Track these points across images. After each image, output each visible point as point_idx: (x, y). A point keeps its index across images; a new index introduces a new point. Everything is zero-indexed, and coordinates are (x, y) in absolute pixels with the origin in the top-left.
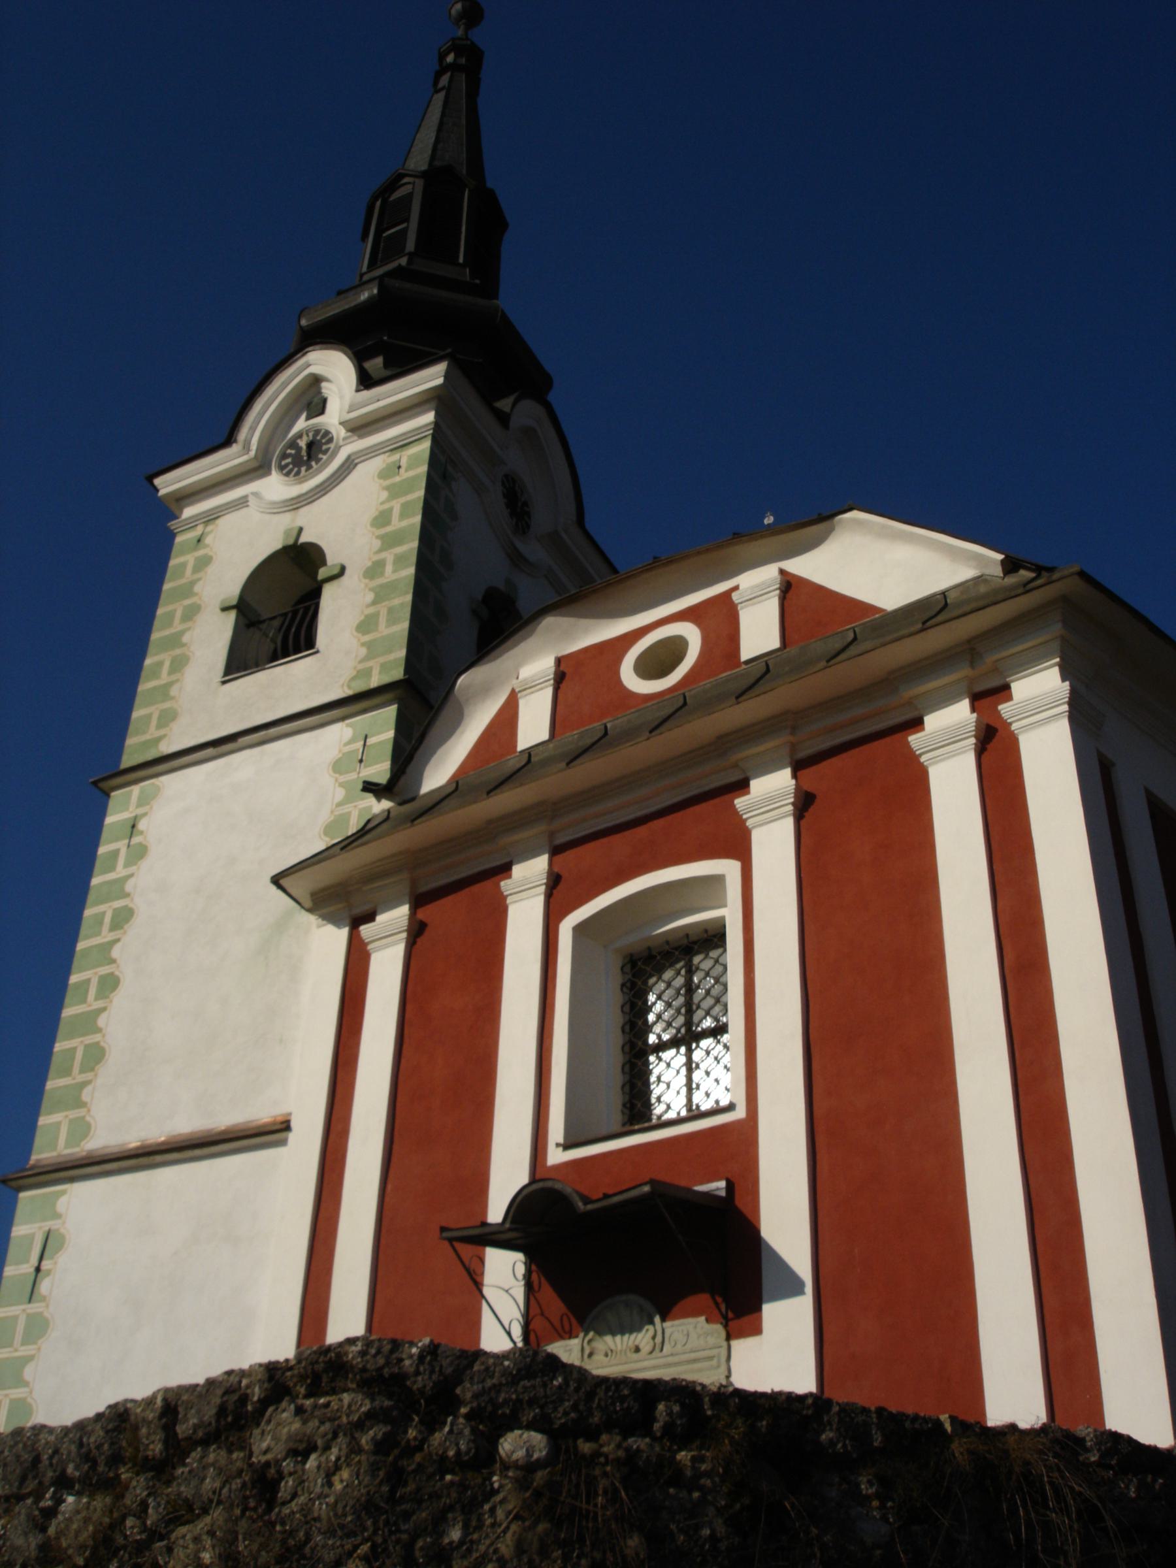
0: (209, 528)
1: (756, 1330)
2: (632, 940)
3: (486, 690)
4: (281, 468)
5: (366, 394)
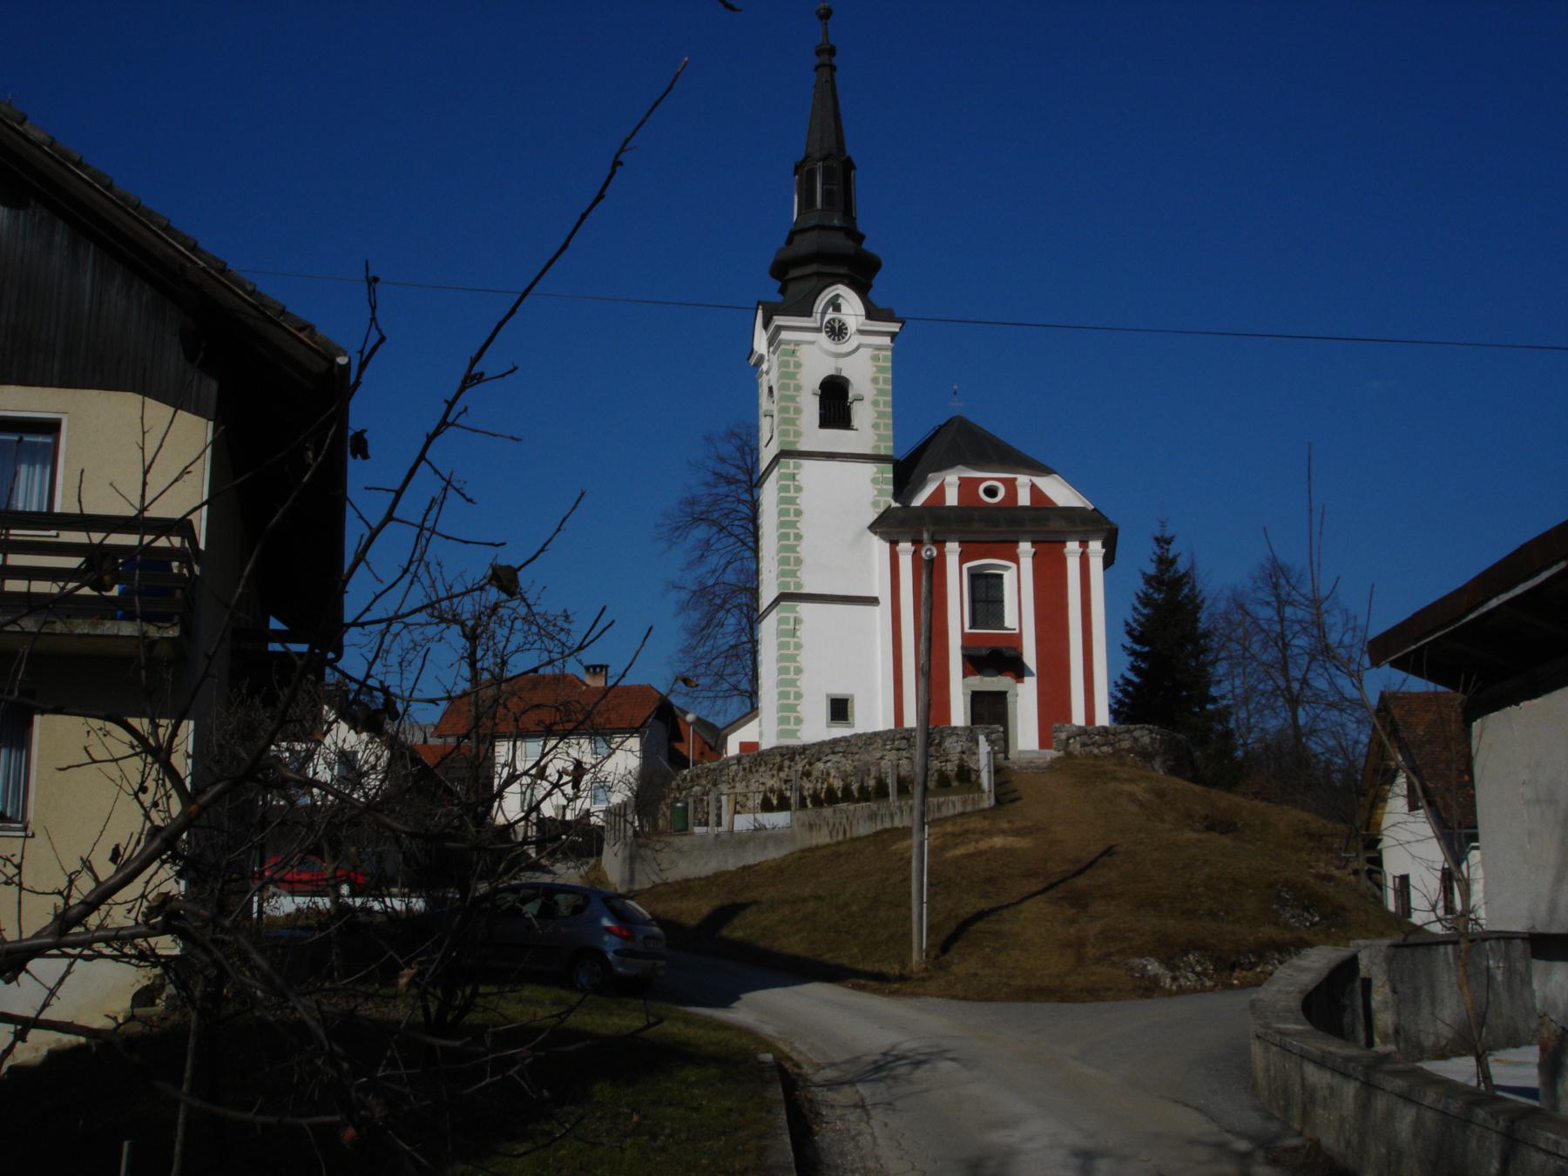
1: (1022, 682)
2: (975, 572)
3: (933, 480)
4: (827, 332)
5: (868, 321)
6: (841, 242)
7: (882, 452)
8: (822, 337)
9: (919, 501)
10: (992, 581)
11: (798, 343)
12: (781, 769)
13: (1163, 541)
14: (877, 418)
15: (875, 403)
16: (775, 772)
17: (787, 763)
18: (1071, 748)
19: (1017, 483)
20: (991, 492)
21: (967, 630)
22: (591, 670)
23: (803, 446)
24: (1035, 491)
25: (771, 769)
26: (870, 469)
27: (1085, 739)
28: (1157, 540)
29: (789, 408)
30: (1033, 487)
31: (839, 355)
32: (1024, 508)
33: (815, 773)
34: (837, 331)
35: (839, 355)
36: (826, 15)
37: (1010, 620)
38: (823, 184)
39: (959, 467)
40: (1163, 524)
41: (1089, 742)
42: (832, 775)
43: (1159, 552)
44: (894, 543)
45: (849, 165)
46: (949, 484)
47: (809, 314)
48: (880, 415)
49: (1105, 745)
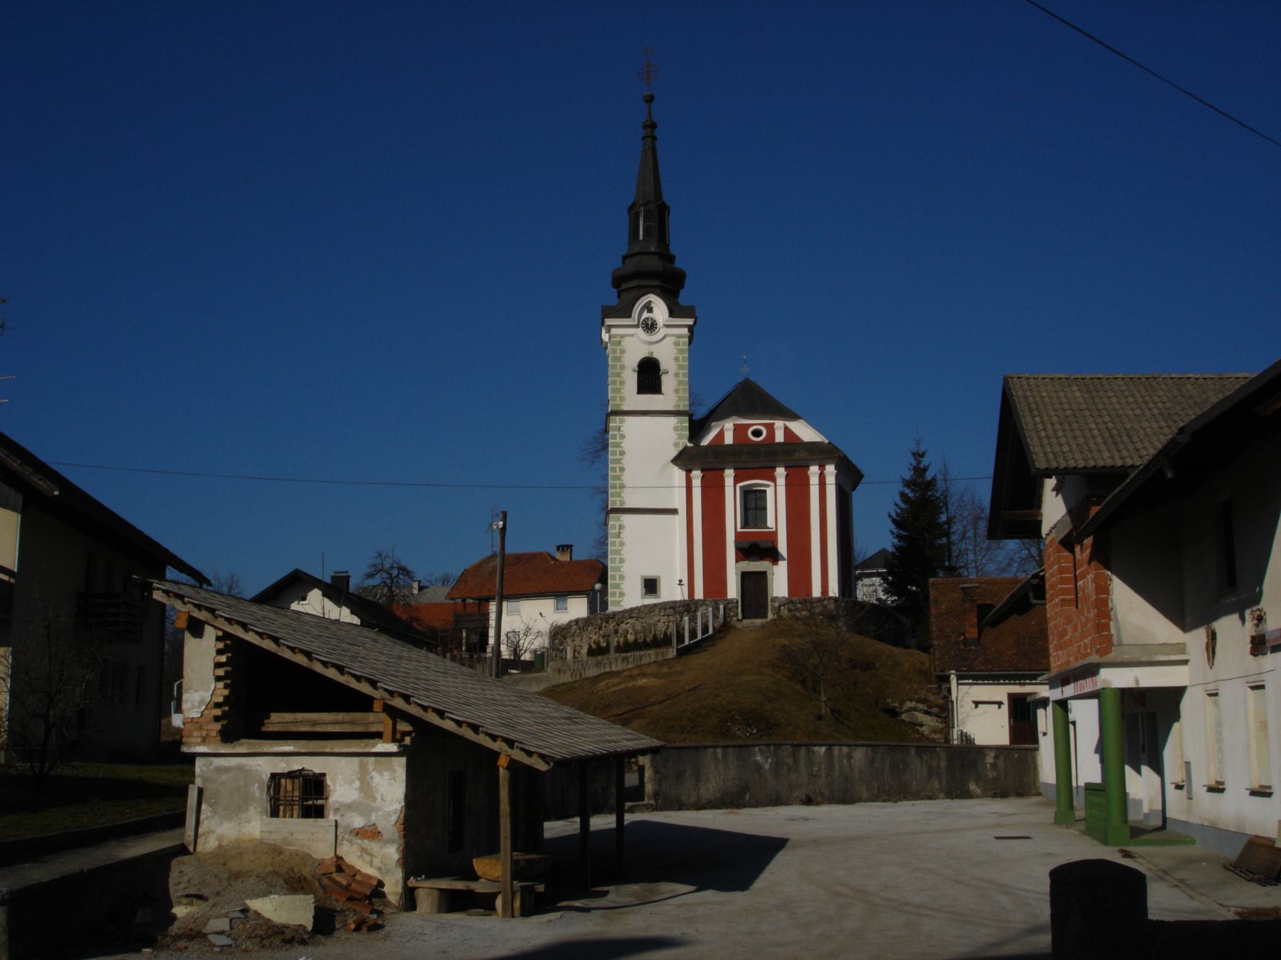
0: (622, 339)
1: (777, 565)
2: (745, 489)
3: (717, 426)
4: (643, 327)
5: (671, 319)
6: (655, 264)
7: (681, 408)
8: (640, 331)
9: (706, 442)
10: (758, 494)
11: (623, 336)
12: (600, 628)
13: (918, 456)
15: (677, 375)
16: (597, 630)
17: (604, 624)
18: (782, 613)
19: (775, 427)
20: (757, 433)
21: (739, 530)
22: (561, 549)
23: (625, 408)
24: (787, 431)
25: (595, 628)
26: (673, 421)
27: (791, 606)
28: (914, 454)
30: (786, 429)
31: (651, 343)
32: (780, 443)
33: (620, 631)
34: (650, 326)
35: (651, 343)
36: (650, 99)
37: (770, 522)
38: (644, 222)
39: (734, 417)
40: (918, 443)
41: (793, 608)
42: (630, 632)
43: (914, 463)
44: (689, 471)
45: (663, 210)
46: (728, 429)
47: (629, 316)
48: (680, 383)
49: (804, 610)
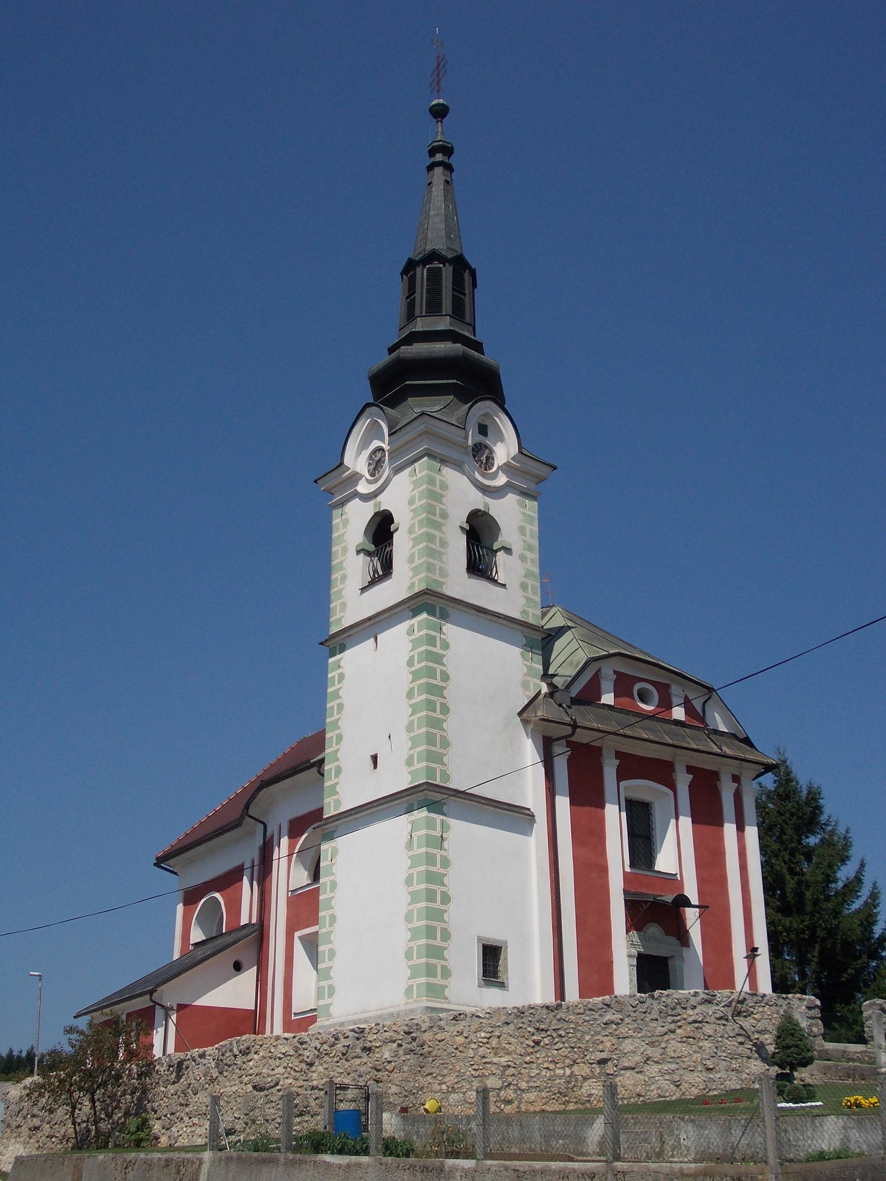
14: (525, 577)
29: (434, 536)
